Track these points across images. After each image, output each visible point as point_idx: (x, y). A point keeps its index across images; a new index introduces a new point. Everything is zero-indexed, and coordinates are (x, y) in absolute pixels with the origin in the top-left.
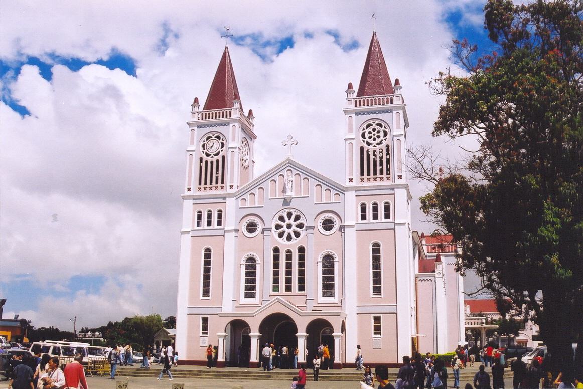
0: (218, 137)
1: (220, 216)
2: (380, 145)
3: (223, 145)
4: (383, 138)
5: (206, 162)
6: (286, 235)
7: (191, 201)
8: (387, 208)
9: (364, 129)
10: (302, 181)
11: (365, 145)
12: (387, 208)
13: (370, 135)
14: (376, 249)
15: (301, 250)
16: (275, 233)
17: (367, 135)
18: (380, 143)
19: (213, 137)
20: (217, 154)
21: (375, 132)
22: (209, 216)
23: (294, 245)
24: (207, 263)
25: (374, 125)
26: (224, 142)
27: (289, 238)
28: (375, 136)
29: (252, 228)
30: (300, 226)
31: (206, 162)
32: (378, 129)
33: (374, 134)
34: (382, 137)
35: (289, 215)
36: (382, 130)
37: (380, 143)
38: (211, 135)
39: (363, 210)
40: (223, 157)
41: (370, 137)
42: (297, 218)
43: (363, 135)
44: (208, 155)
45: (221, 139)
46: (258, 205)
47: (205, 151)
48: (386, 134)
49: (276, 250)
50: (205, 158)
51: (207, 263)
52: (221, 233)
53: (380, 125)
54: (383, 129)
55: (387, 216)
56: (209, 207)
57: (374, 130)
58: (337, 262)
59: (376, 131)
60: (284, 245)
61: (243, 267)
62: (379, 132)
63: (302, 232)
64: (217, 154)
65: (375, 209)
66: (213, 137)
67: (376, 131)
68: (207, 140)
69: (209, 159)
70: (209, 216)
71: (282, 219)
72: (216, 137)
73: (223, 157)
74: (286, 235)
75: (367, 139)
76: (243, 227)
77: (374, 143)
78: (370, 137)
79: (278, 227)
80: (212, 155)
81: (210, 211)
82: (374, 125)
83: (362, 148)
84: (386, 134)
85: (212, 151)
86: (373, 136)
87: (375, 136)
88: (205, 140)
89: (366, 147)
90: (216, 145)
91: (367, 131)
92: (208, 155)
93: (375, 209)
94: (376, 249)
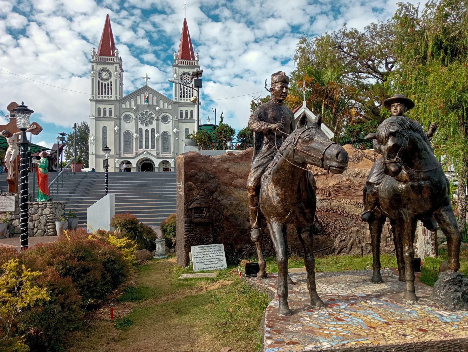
5: (102, 83)
20: (107, 79)
31: (102, 83)
40: (111, 82)
43: (181, 78)
44: (102, 79)
55: (192, 117)
60: (144, 128)
62: (189, 78)
64: (107, 79)
69: (104, 83)
73: (111, 82)
92: (102, 79)
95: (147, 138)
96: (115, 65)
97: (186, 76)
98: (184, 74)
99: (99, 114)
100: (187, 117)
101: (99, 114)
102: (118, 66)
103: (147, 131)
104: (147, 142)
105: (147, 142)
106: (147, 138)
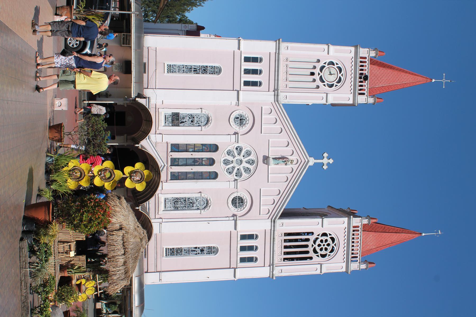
0: (339, 81)
1: (255, 84)
2: (312, 252)
3: (331, 86)
4: (319, 254)
6: (230, 158)
7: (273, 51)
8: (250, 259)
9: (330, 235)
10: (285, 175)
11: (315, 236)
12: (250, 259)
13: (324, 241)
14: (212, 251)
15: (214, 176)
16: (232, 147)
17: (324, 238)
18: (315, 251)
19: (340, 75)
20: (322, 80)
21: (326, 246)
22: (255, 72)
23: (218, 167)
24: (204, 70)
25: (333, 245)
26: (334, 87)
27: (226, 162)
28: (322, 244)
29: (241, 120)
30: (239, 174)
32: (328, 249)
33: (324, 245)
34: (320, 253)
35: (251, 162)
36: (328, 252)
37: (315, 251)
38: (343, 72)
39: (251, 237)
41: (322, 241)
42: (247, 170)
45: (337, 84)
46: (264, 108)
47: (326, 65)
48: (323, 256)
49: (214, 148)
50: (319, 66)
51: (204, 70)
52: (237, 87)
53: (332, 251)
54: (328, 254)
55: (243, 260)
56: (265, 72)
57: (328, 245)
58: (200, 213)
59: (327, 247)
61: (198, 112)
62: (326, 249)
63: (233, 176)
64: (322, 80)
65: (251, 248)
66: (340, 75)
67: (327, 247)
68: (338, 67)
69: (317, 71)
70: (255, 72)
71: (248, 153)
72: (340, 78)
74: (230, 158)
75: (321, 238)
76: (241, 111)
77: (316, 246)
78: (322, 241)
79: (239, 150)
80: (321, 74)
81: (261, 72)
82: (333, 245)
83: (312, 233)
84: (323, 256)
85: (325, 74)
86: (322, 244)
87: (322, 246)
88: (338, 66)
89: (312, 238)
90: (332, 79)
91: (328, 238)
93: (251, 248)
94: (212, 251)
95: (195, 162)
96: (351, 96)
97: (328, 245)
98: (333, 239)
99: (247, 59)
100: (243, 249)
101: (247, 59)
102: (351, 102)
103: (211, 162)
104: (186, 162)
105: (186, 162)
106: (195, 162)
